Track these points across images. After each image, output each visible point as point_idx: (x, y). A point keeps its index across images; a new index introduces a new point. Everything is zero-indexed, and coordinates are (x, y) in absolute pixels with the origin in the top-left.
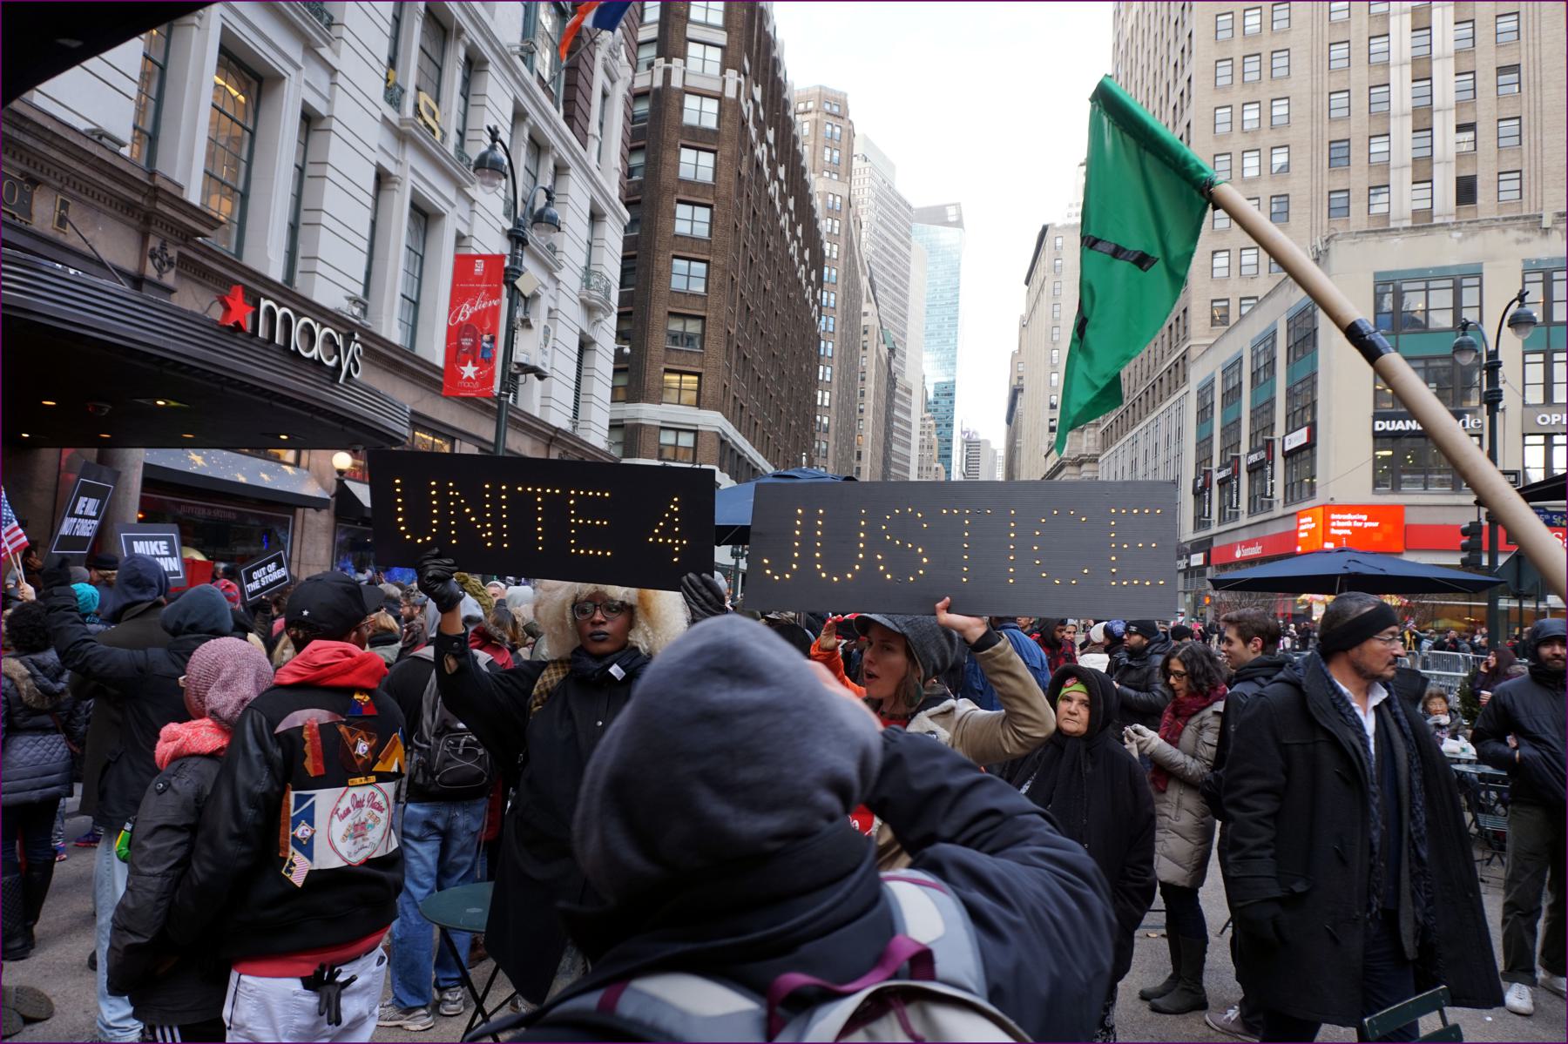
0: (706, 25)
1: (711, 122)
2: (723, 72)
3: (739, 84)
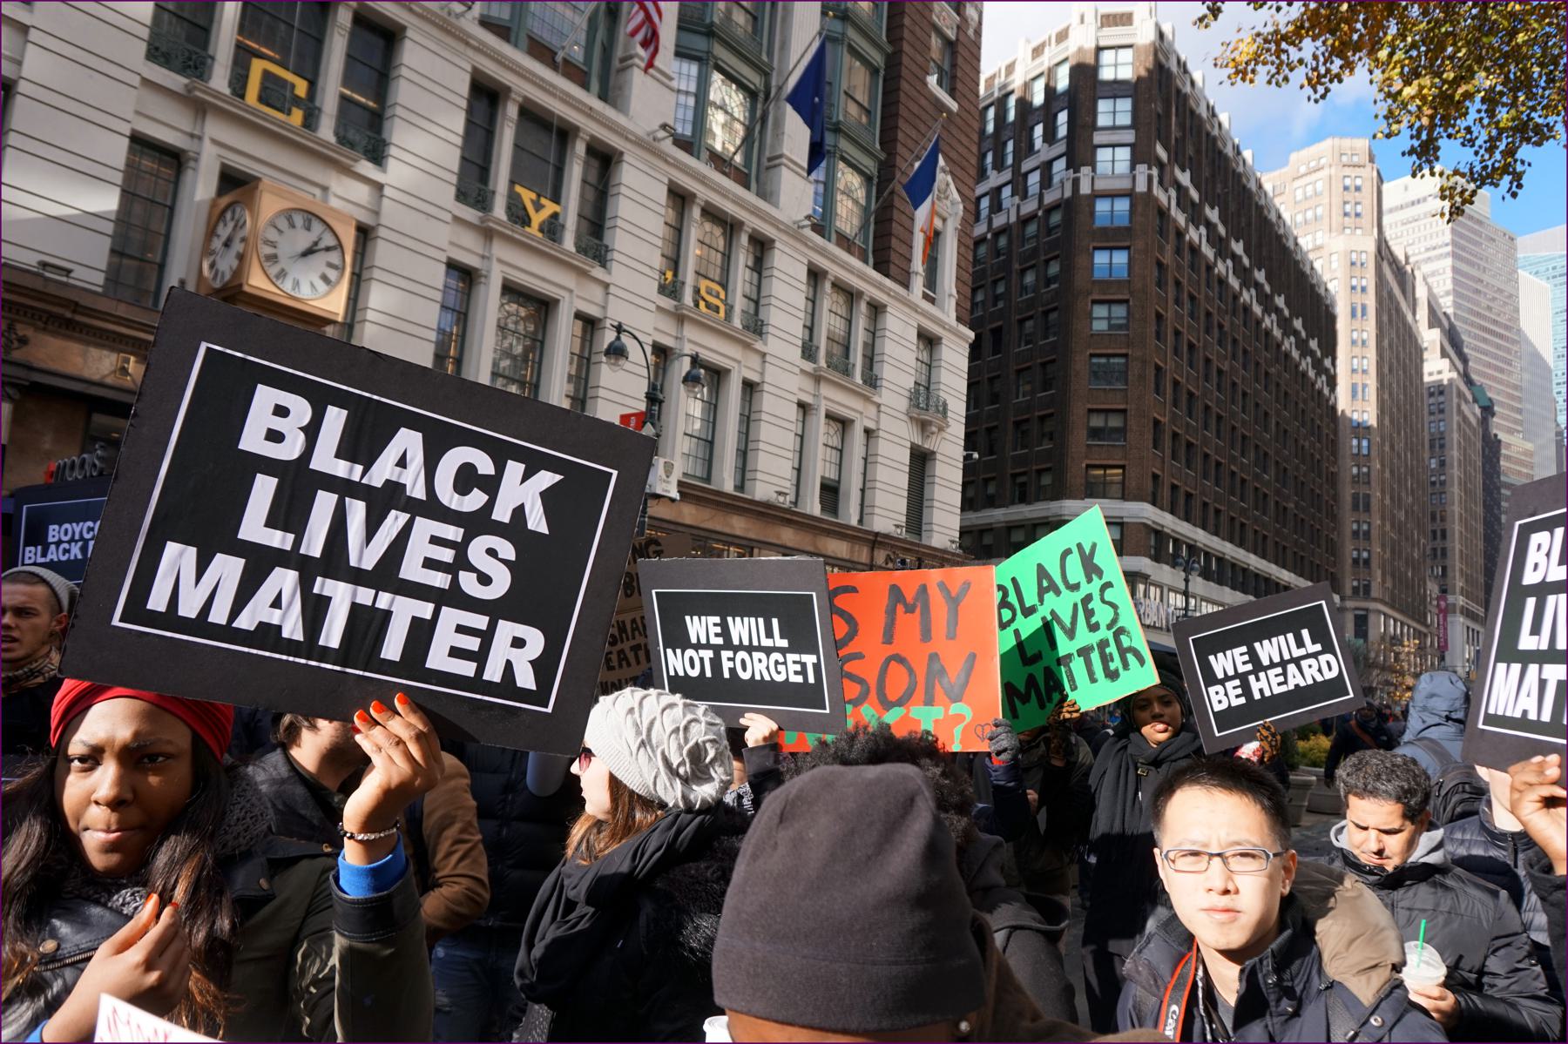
0: (1114, 128)
2: (1133, 168)
3: (1150, 178)
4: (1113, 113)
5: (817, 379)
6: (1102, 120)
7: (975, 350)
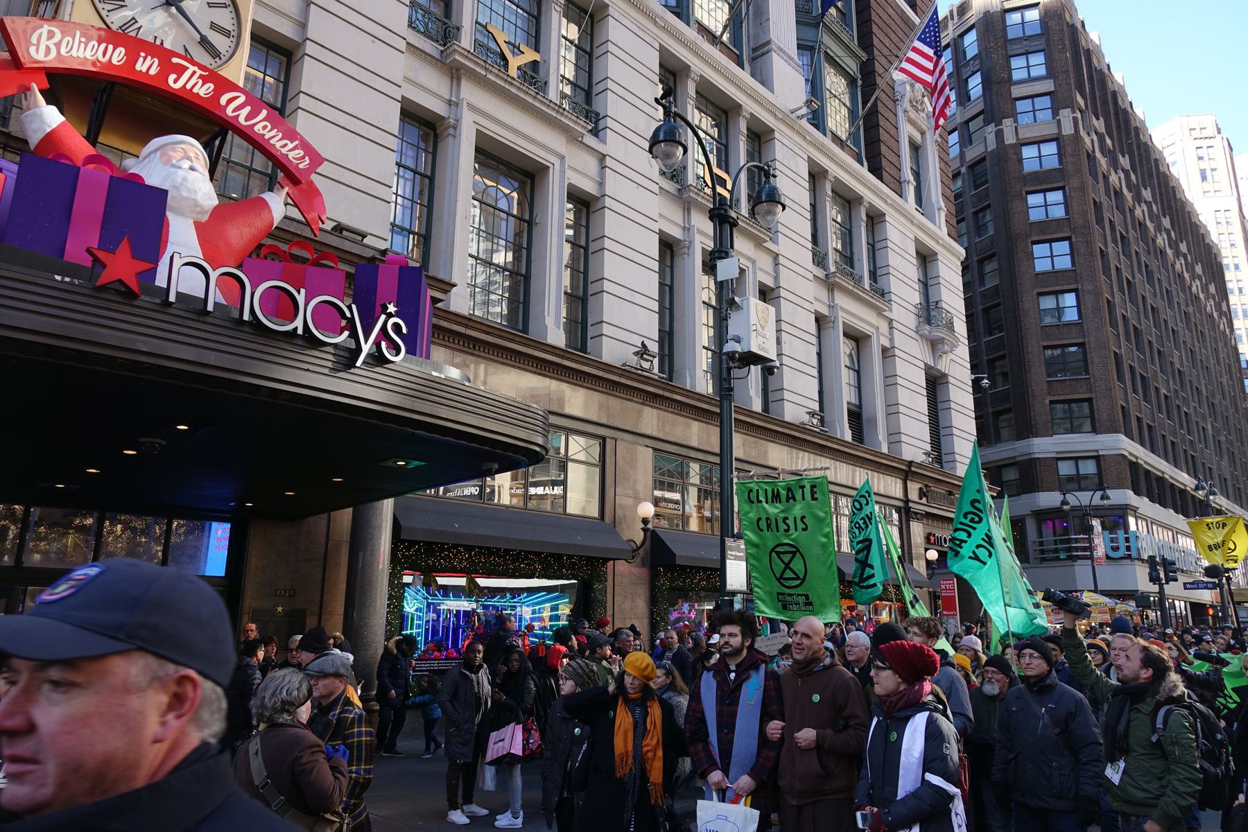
0: (1031, 80)
1: (1052, 163)
2: (1055, 113)
4: (1028, 68)
5: (830, 285)
6: (1017, 75)
7: (966, 268)
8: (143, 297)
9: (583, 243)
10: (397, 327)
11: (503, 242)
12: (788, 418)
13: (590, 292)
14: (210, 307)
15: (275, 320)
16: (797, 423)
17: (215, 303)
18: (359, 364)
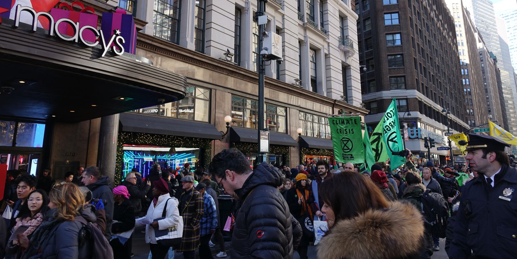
5: (305, 28)
7: (358, 23)
8: (3, 24)
9: (203, 7)
10: (120, 40)
11: (169, 6)
12: (287, 82)
13: (206, 28)
14: (35, 29)
15: (65, 35)
16: (291, 84)
17: (37, 28)
18: (103, 55)
